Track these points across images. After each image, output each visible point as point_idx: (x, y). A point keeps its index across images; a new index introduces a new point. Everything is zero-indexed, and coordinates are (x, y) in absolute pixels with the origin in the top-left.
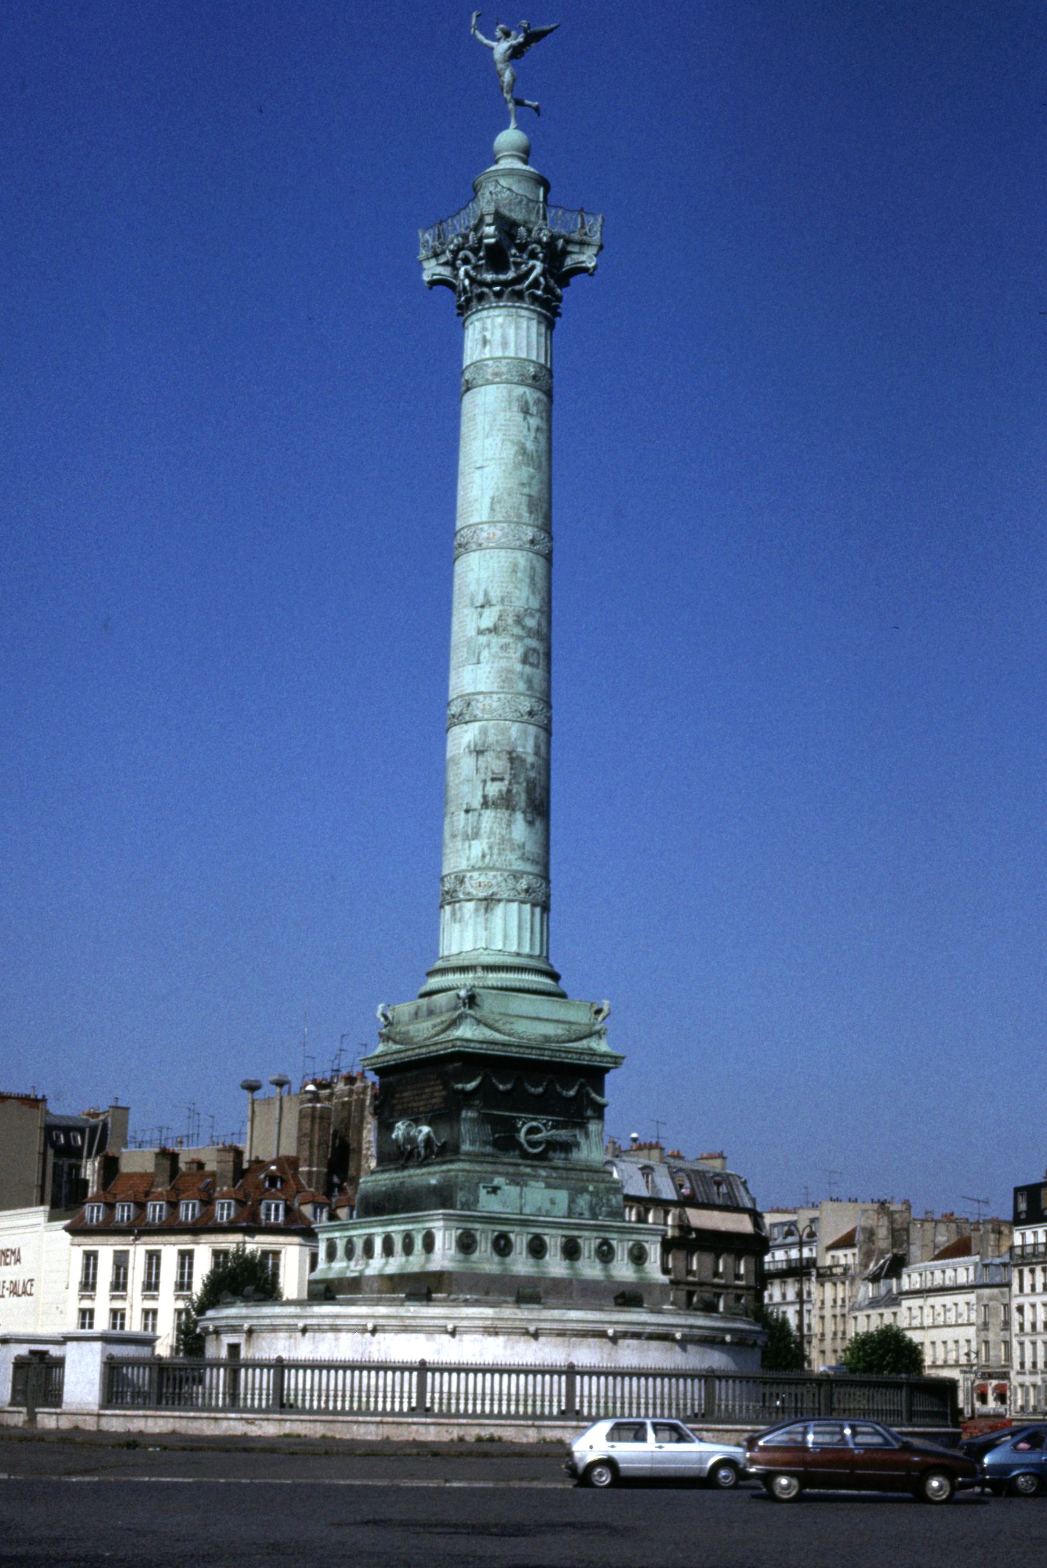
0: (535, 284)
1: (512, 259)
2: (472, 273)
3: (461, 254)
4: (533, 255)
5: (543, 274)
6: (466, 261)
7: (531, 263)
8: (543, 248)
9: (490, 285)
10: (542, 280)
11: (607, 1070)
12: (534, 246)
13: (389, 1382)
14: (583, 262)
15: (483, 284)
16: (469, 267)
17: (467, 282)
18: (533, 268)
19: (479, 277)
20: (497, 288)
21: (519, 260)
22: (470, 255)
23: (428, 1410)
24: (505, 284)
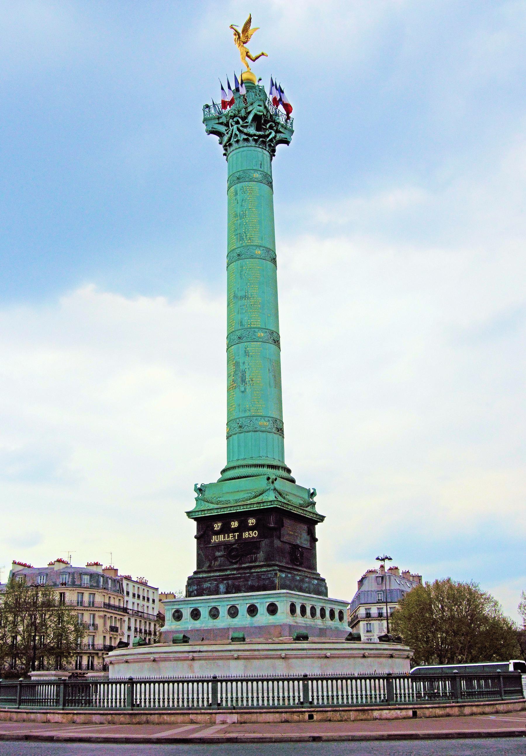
2: (241, 128)
3: (235, 119)
4: (271, 127)
6: (237, 123)
7: (270, 131)
8: (275, 125)
9: (251, 136)
11: (316, 522)
13: (382, 685)
15: (246, 134)
16: (239, 126)
17: (238, 133)
18: (270, 133)
19: (245, 130)
20: (255, 138)
22: (240, 120)
23: (219, 705)
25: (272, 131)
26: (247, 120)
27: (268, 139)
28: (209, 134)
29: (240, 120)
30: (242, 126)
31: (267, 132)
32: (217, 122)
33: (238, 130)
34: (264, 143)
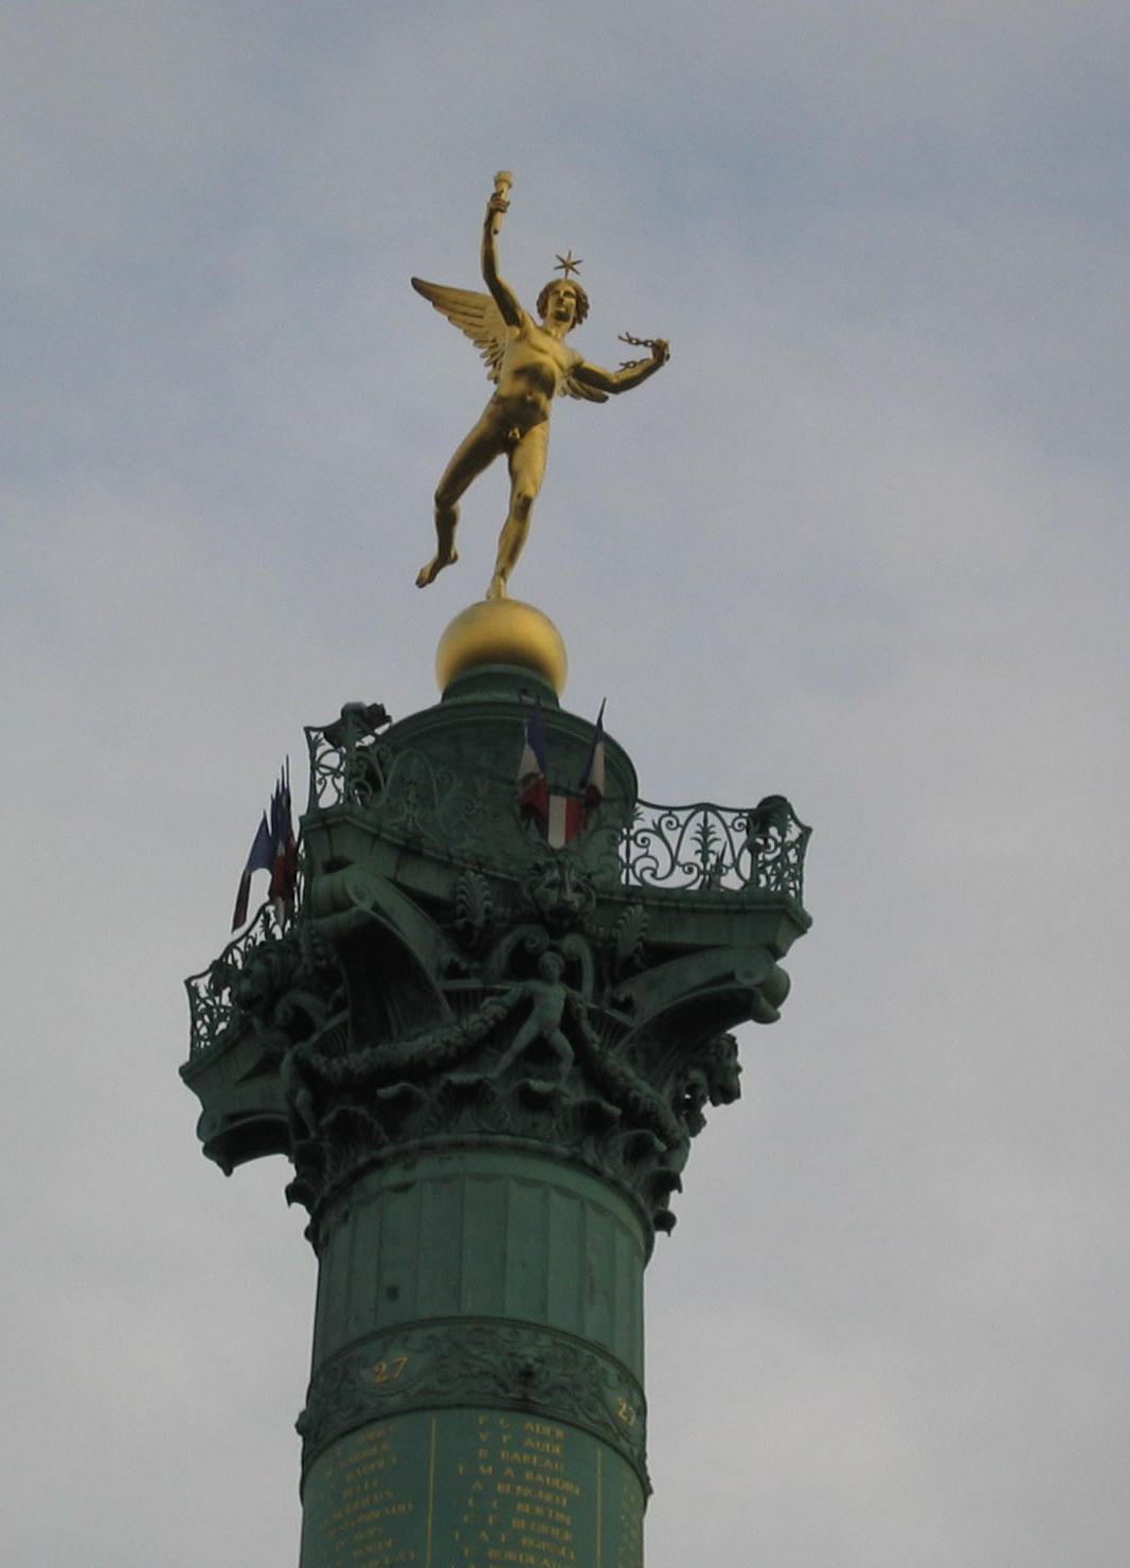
0: (540, 1051)
1: (440, 985)
2: (318, 1061)
3: (282, 1010)
4: (524, 965)
5: (569, 1024)
6: (299, 1026)
7: (515, 989)
10: (561, 1041)
12: (522, 930)
14: (730, 977)
18: (523, 1009)
21: (474, 983)
22: (307, 1000)
24: (420, 1071)
25: (535, 985)
26: (339, 991)
27: (506, 1059)
28: (228, 1172)
29: (307, 1000)
30: (323, 1048)
31: (492, 1009)
32: (247, 1059)
33: (305, 1071)
34: (474, 1095)
